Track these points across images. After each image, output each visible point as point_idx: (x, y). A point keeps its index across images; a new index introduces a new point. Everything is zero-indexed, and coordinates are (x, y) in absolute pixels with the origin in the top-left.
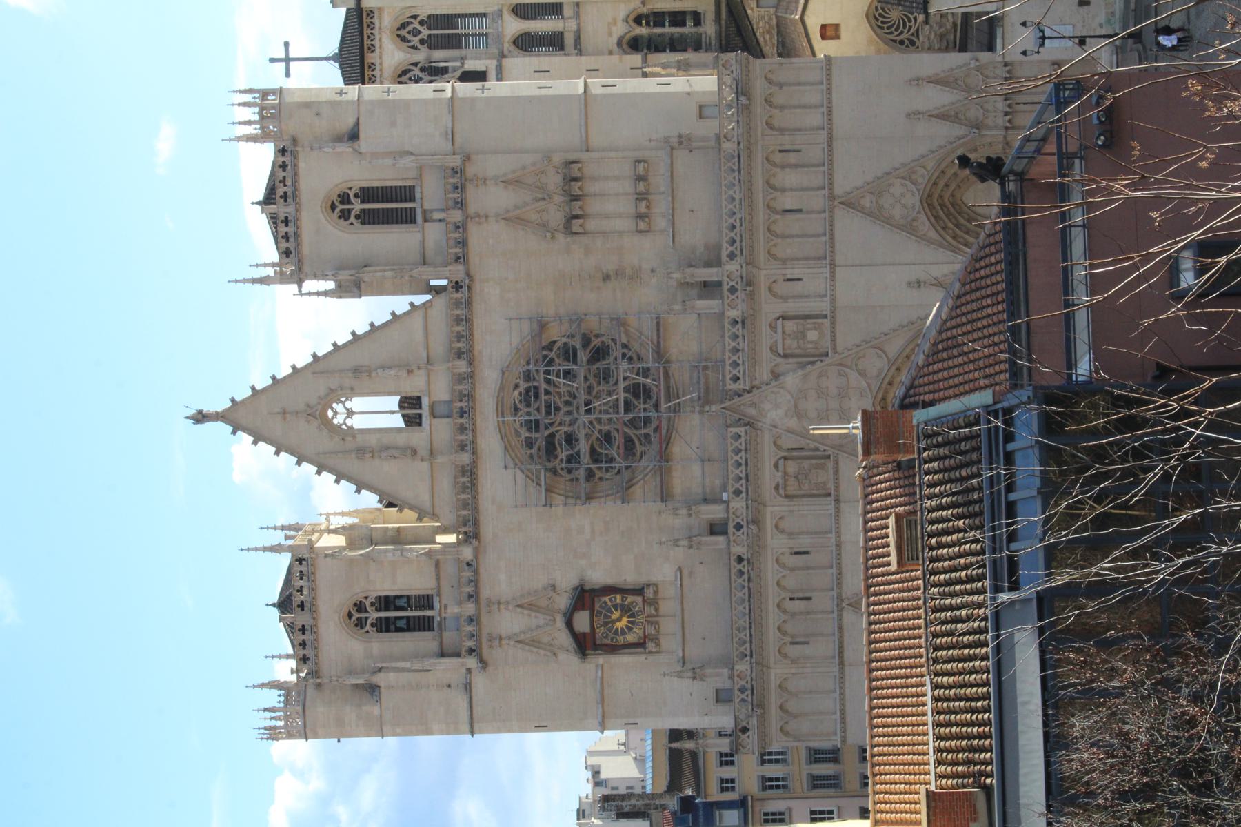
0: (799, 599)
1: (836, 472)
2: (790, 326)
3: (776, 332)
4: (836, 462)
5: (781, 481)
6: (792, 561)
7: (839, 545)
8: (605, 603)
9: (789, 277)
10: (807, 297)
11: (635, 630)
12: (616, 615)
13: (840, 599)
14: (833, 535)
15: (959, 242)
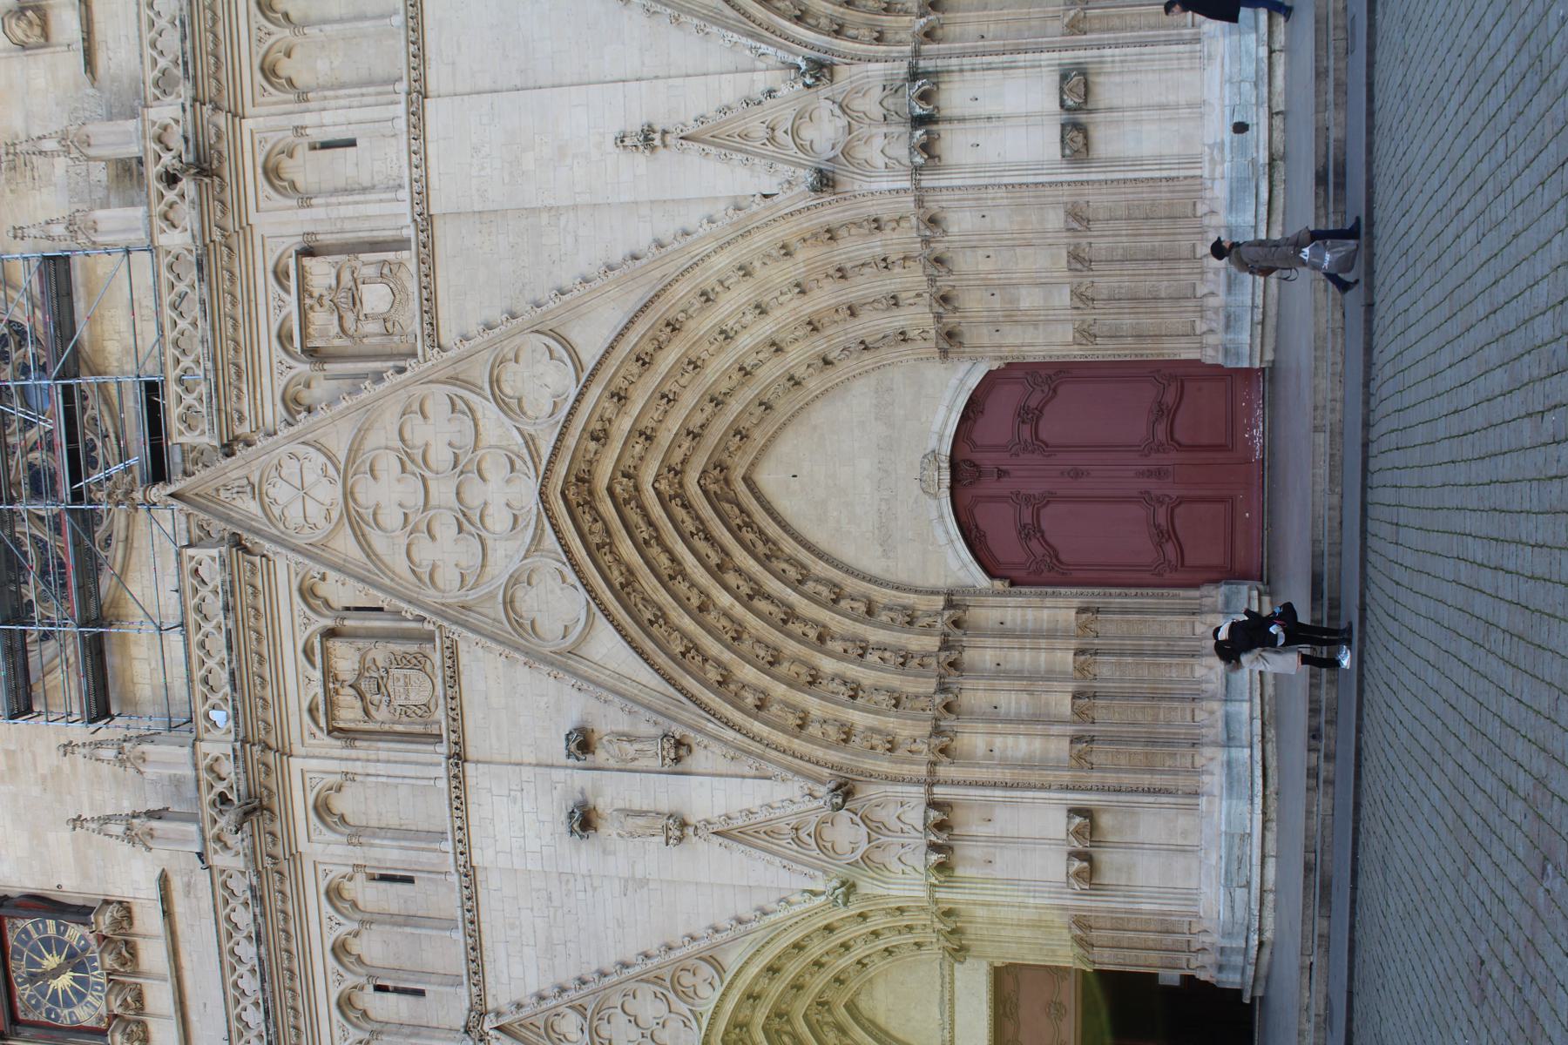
0: (397, 990)
1: (453, 677)
2: (321, 272)
3: (287, 291)
4: (452, 654)
5: (320, 691)
6: (371, 896)
7: (469, 874)
8: (25, 931)
9: (318, 136)
10: (371, 189)
11: (89, 998)
12: (51, 961)
13: (479, 1011)
14: (448, 846)
15: (778, 11)
